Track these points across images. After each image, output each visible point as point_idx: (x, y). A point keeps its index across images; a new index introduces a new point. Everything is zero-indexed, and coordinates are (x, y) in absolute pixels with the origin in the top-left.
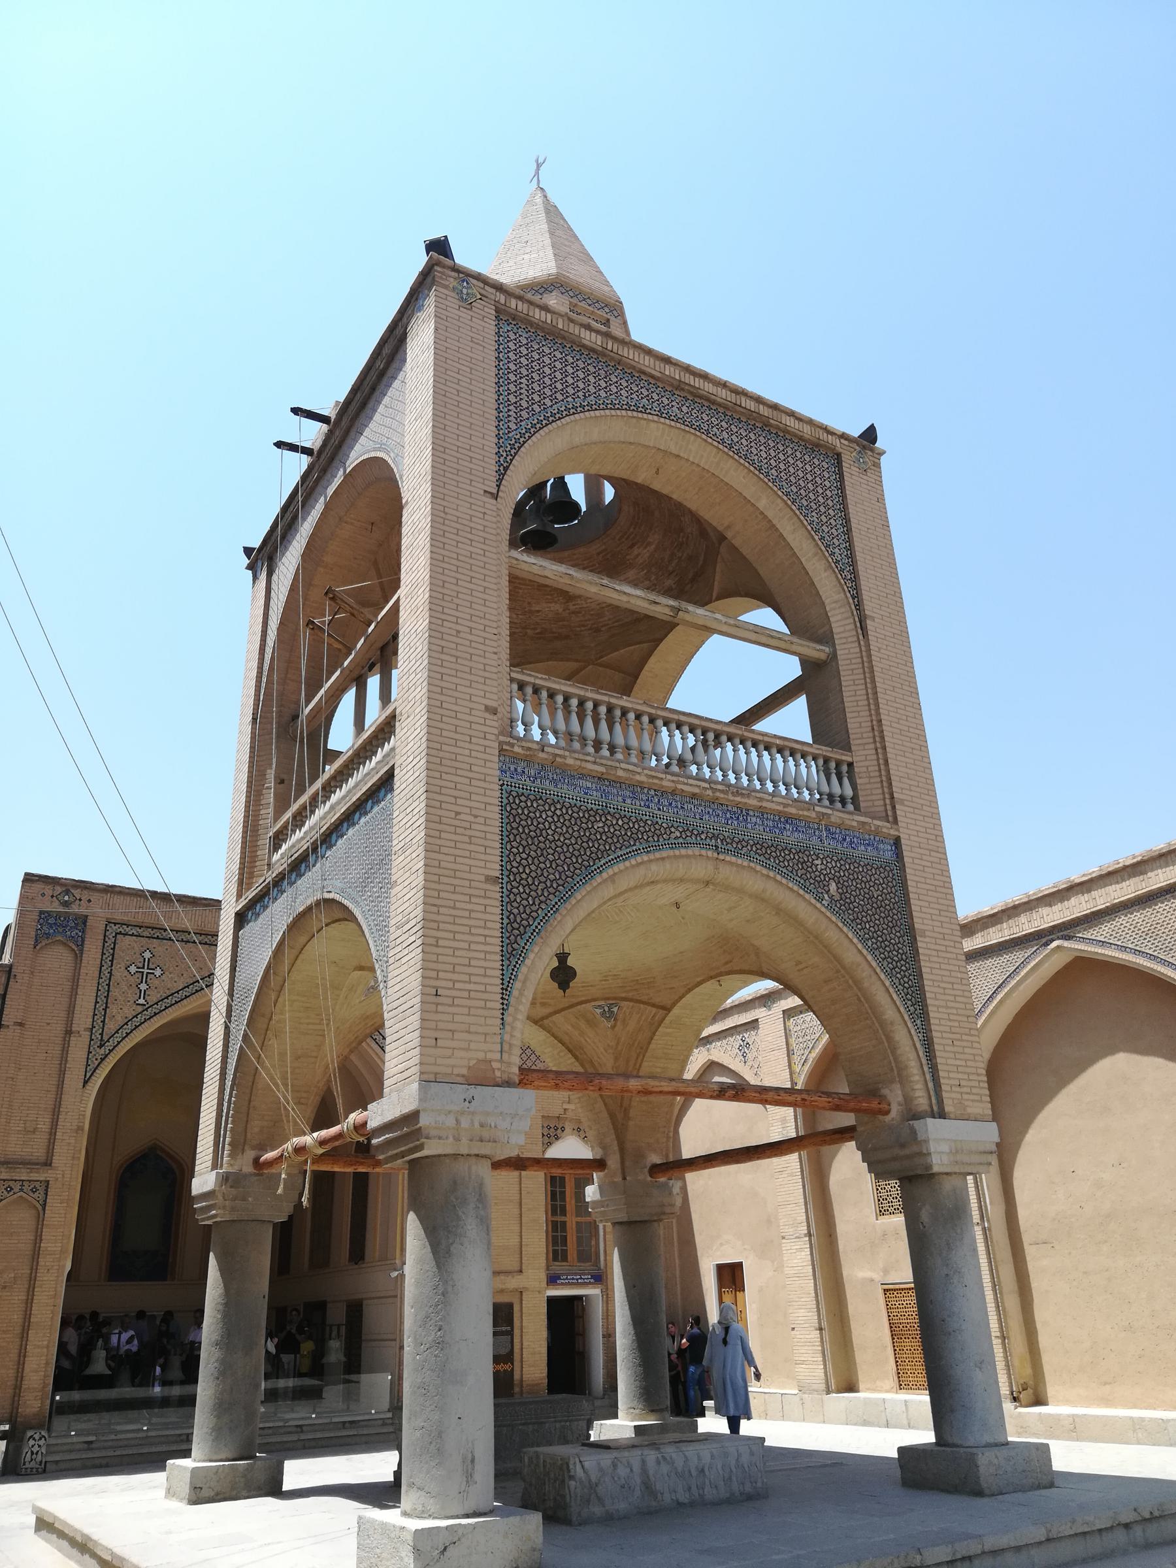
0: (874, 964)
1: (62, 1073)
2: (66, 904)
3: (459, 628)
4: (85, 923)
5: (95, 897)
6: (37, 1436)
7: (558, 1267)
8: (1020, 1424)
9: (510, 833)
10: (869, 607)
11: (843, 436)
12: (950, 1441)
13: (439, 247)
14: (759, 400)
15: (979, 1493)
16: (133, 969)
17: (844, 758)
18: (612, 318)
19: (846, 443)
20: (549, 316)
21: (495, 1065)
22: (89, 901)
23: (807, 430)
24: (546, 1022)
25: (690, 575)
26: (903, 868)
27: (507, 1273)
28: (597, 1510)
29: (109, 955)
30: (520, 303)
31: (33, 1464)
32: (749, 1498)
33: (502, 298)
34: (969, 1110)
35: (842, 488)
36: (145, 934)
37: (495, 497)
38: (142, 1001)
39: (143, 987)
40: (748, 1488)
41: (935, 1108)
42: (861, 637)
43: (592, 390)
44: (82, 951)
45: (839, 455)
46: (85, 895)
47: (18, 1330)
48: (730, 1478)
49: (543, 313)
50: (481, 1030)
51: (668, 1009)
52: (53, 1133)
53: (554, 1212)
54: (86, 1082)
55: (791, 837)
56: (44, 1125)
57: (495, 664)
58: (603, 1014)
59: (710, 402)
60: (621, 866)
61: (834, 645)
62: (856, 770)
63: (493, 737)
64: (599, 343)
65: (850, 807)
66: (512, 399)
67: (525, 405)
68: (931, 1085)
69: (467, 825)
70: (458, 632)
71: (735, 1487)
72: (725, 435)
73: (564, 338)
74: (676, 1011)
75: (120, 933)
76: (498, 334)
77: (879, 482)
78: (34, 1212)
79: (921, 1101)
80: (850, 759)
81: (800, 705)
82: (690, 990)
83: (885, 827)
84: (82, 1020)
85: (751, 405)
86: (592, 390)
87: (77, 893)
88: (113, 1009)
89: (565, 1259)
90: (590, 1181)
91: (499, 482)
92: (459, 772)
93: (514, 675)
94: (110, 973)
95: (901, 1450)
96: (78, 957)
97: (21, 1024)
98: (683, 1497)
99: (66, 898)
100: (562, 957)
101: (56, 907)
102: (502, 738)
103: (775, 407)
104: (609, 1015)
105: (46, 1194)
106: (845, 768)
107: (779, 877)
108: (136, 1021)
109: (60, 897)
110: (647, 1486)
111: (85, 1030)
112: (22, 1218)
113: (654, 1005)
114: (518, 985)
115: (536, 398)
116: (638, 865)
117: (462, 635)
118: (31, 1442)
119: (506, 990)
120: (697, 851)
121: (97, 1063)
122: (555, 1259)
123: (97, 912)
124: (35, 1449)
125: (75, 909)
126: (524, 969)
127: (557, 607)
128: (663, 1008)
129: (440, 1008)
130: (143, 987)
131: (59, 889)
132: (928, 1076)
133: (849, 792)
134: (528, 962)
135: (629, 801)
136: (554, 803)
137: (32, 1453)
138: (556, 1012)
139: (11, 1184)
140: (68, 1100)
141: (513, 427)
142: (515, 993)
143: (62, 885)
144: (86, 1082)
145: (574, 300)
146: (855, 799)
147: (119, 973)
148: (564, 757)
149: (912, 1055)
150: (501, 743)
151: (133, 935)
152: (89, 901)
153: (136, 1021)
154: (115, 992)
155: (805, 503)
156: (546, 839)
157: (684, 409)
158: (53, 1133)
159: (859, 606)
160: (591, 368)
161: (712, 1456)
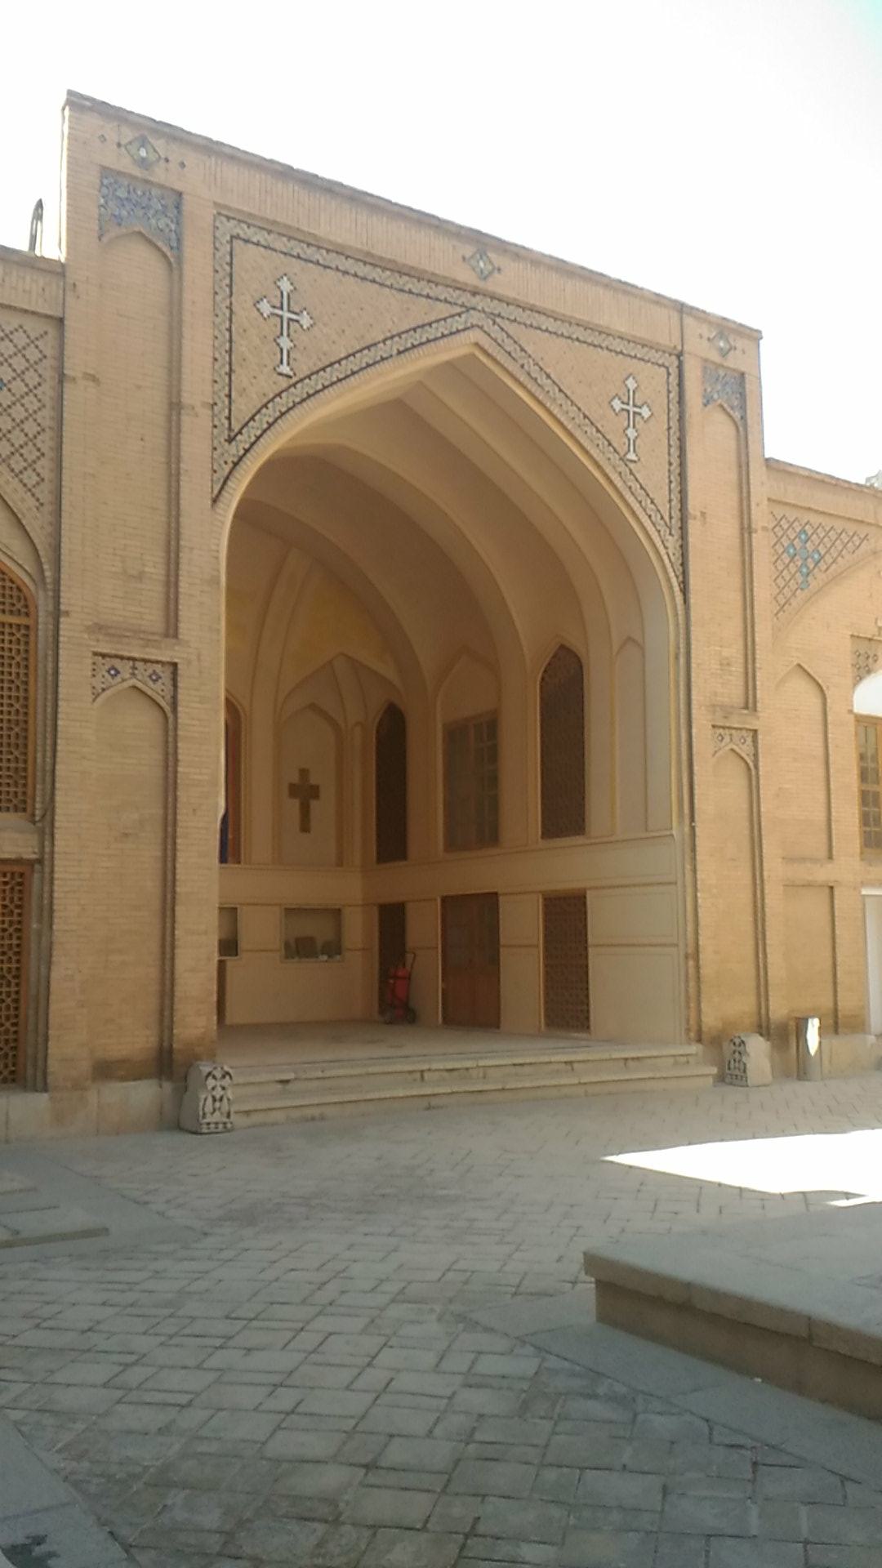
2: (143, 163)
5: (191, 158)
6: (218, 1074)
16: (265, 307)
31: (217, 1117)
36: (278, 245)
38: (285, 369)
46: (176, 153)
47: (156, 904)
52: (172, 582)
54: (215, 501)
56: (155, 568)
75: (238, 237)
78: (157, 714)
87: (160, 144)
88: (241, 378)
94: (230, 308)
97: (94, 379)
99: (143, 153)
101: (125, 164)
105: (175, 686)
109: (133, 150)
111: (204, 404)
118: (211, 1082)
121: (227, 469)
124: (218, 1093)
125: (159, 175)
130: (285, 343)
131: (128, 134)
137: (214, 1100)
139: (117, 663)
144: (215, 501)
151: (258, 244)
152: (183, 165)
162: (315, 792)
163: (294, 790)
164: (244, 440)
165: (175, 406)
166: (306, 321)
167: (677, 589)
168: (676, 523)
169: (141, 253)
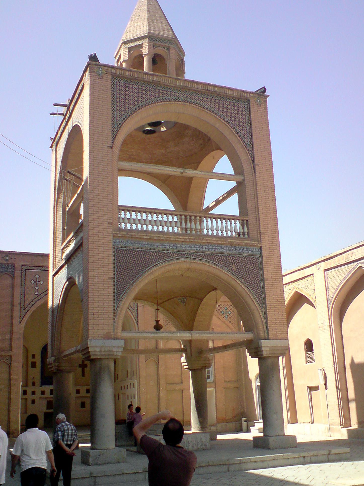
0: (247, 291)
1: (12, 320)
2: (7, 260)
3: (99, 197)
4: (14, 266)
8: (290, 430)
9: (117, 262)
10: (256, 162)
12: (267, 435)
14: (215, 86)
15: (269, 449)
17: (244, 219)
18: (170, 46)
19: (252, 95)
20: (132, 73)
21: (112, 333)
22: (15, 258)
23: (235, 93)
24: (162, 305)
25: (207, 140)
26: (262, 257)
27: (177, 384)
29: (24, 277)
30: (121, 71)
32: (204, 450)
33: (114, 71)
34: (279, 337)
35: (250, 114)
38: (37, 293)
39: (37, 288)
40: (204, 447)
41: (266, 336)
42: (253, 173)
43: (149, 97)
44: (14, 277)
45: (249, 100)
48: (198, 444)
49: (129, 73)
50: (107, 324)
51: (202, 300)
54: (20, 322)
56: (8, 337)
57: (111, 207)
58: (182, 301)
59: (196, 92)
60: (155, 268)
61: (244, 176)
62: (249, 222)
63: (111, 232)
64: (151, 79)
65: (246, 236)
66: (118, 108)
67: (123, 109)
68: (265, 329)
69: (102, 262)
70: (99, 198)
71: (199, 447)
72: (201, 102)
73: (137, 80)
74: (205, 300)
76: (113, 84)
77: (266, 109)
79: (262, 335)
80: (247, 219)
81: (235, 197)
82: (208, 294)
84: (17, 300)
85: (212, 89)
86: (149, 97)
87: (10, 256)
88: (27, 296)
90: (182, 356)
92: (100, 245)
93: (120, 208)
95: (253, 437)
96: (13, 278)
99: (7, 258)
102: (114, 232)
103: (222, 87)
104: (183, 302)
106: (245, 222)
107: (213, 266)
108: (36, 300)
112: (4, 368)
113: (197, 298)
114: (119, 309)
115: (127, 106)
116: (161, 267)
117: (100, 199)
119: (115, 311)
120: (183, 260)
123: (19, 262)
125: (11, 262)
126: (121, 304)
127: (163, 151)
128: (200, 299)
129: (95, 318)
130: (37, 288)
131: (4, 255)
132: (265, 327)
133: (246, 230)
134: (123, 302)
135: (159, 247)
136: (132, 250)
138: (165, 301)
140: (15, 329)
141: (118, 119)
142: (119, 312)
143: (5, 253)
144: (20, 322)
145: (156, 42)
146: (248, 233)
147: (28, 283)
148: (135, 235)
149: (260, 320)
150: (113, 234)
153: (36, 300)
154: (27, 291)
155: (234, 123)
156: (129, 263)
157: (185, 96)
158: (11, 340)
159: (253, 161)
160: (148, 89)
161: (192, 438)
162: (86, 366)
163: (80, 366)
164: (27, 309)
165: (13, 305)
166: (41, 282)
167: (136, 323)
168: (136, 309)
169: (7, 277)
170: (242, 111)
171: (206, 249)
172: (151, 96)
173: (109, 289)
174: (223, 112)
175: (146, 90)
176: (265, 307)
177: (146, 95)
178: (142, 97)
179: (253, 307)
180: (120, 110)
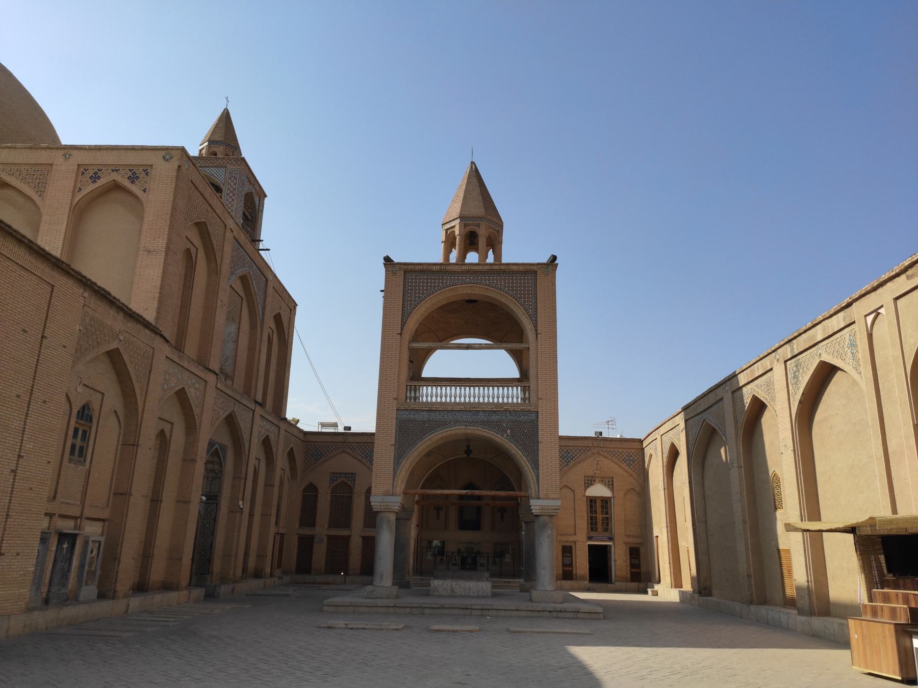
7: (592, 534)
11: (538, 264)
13: (387, 260)
23: (521, 268)
28: (437, 593)
37: (401, 334)
53: (591, 512)
55: (495, 418)
79: (534, 494)
83: (532, 409)
89: (596, 530)
91: (402, 329)
98: (463, 594)
100: (468, 447)
110: (452, 590)
122: (592, 529)
159: (536, 330)
170: (528, 283)
171: (481, 416)
172: (439, 283)
173: (391, 453)
174: (508, 287)
175: (435, 279)
176: (538, 469)
177: (435, 283)
178: (431, 286)
179: (526, 468)
180: (411, 301)
